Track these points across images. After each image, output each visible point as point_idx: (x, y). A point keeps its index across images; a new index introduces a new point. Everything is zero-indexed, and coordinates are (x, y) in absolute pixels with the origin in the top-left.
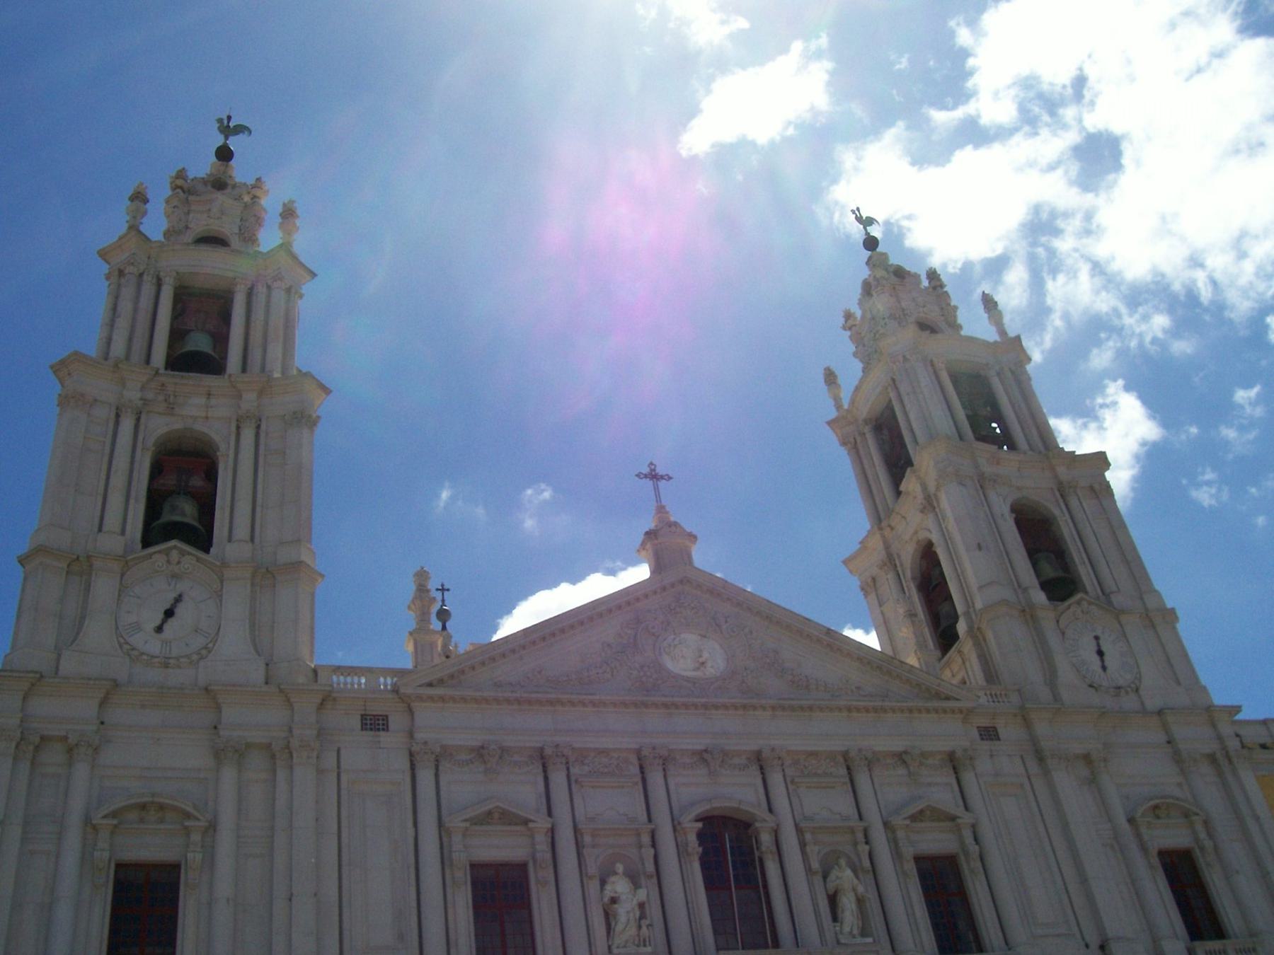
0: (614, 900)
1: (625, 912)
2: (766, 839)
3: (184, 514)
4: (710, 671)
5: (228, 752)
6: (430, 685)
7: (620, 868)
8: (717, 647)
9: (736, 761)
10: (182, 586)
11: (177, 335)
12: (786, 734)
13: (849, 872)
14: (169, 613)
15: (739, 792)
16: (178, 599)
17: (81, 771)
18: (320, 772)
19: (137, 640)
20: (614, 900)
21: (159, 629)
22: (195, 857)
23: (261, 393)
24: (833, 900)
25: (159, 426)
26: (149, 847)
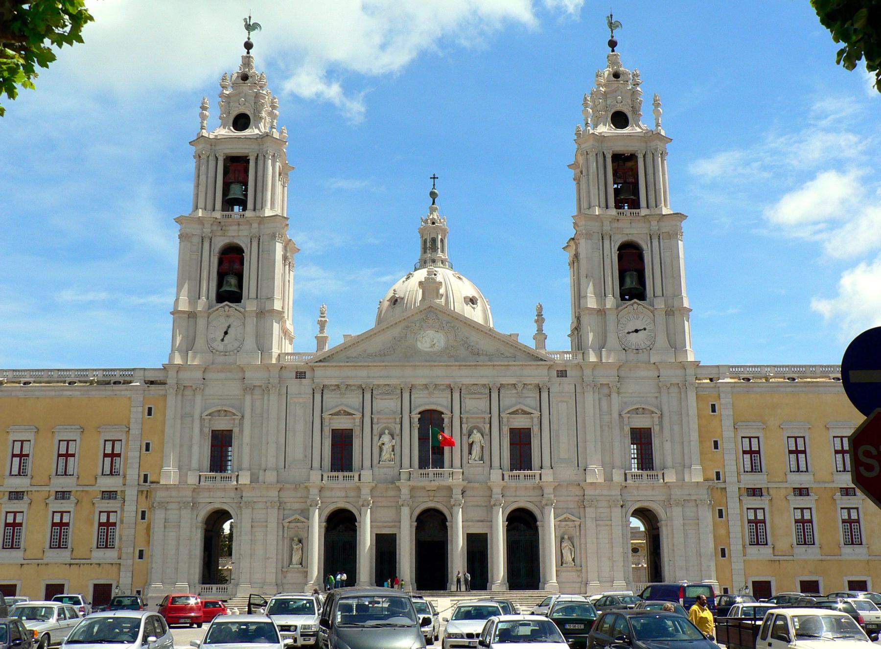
0: (383, 444)
1: (387, 448)
2: (446, 421)
3: (231, 285)
4: (437, 348)
5: (249, 389)
6: (320, 361)
7: (387, 432)
8: (442, 337)
9: (442, 387)
10: (230, 320)
11: (226, 191)
12: (465, 377)
13: (479, 435)
14: (226, 333)
15: (439, 402)
16: (229, 327)
17: (198, 399)
18: (279, 394)
19: (215, 345)
20: (383, 444)
21: (223, 340)
22: (236, 431)
23: (259, 224)
24: (471, 445)
25: (220, 242)
26: (222, 425)
